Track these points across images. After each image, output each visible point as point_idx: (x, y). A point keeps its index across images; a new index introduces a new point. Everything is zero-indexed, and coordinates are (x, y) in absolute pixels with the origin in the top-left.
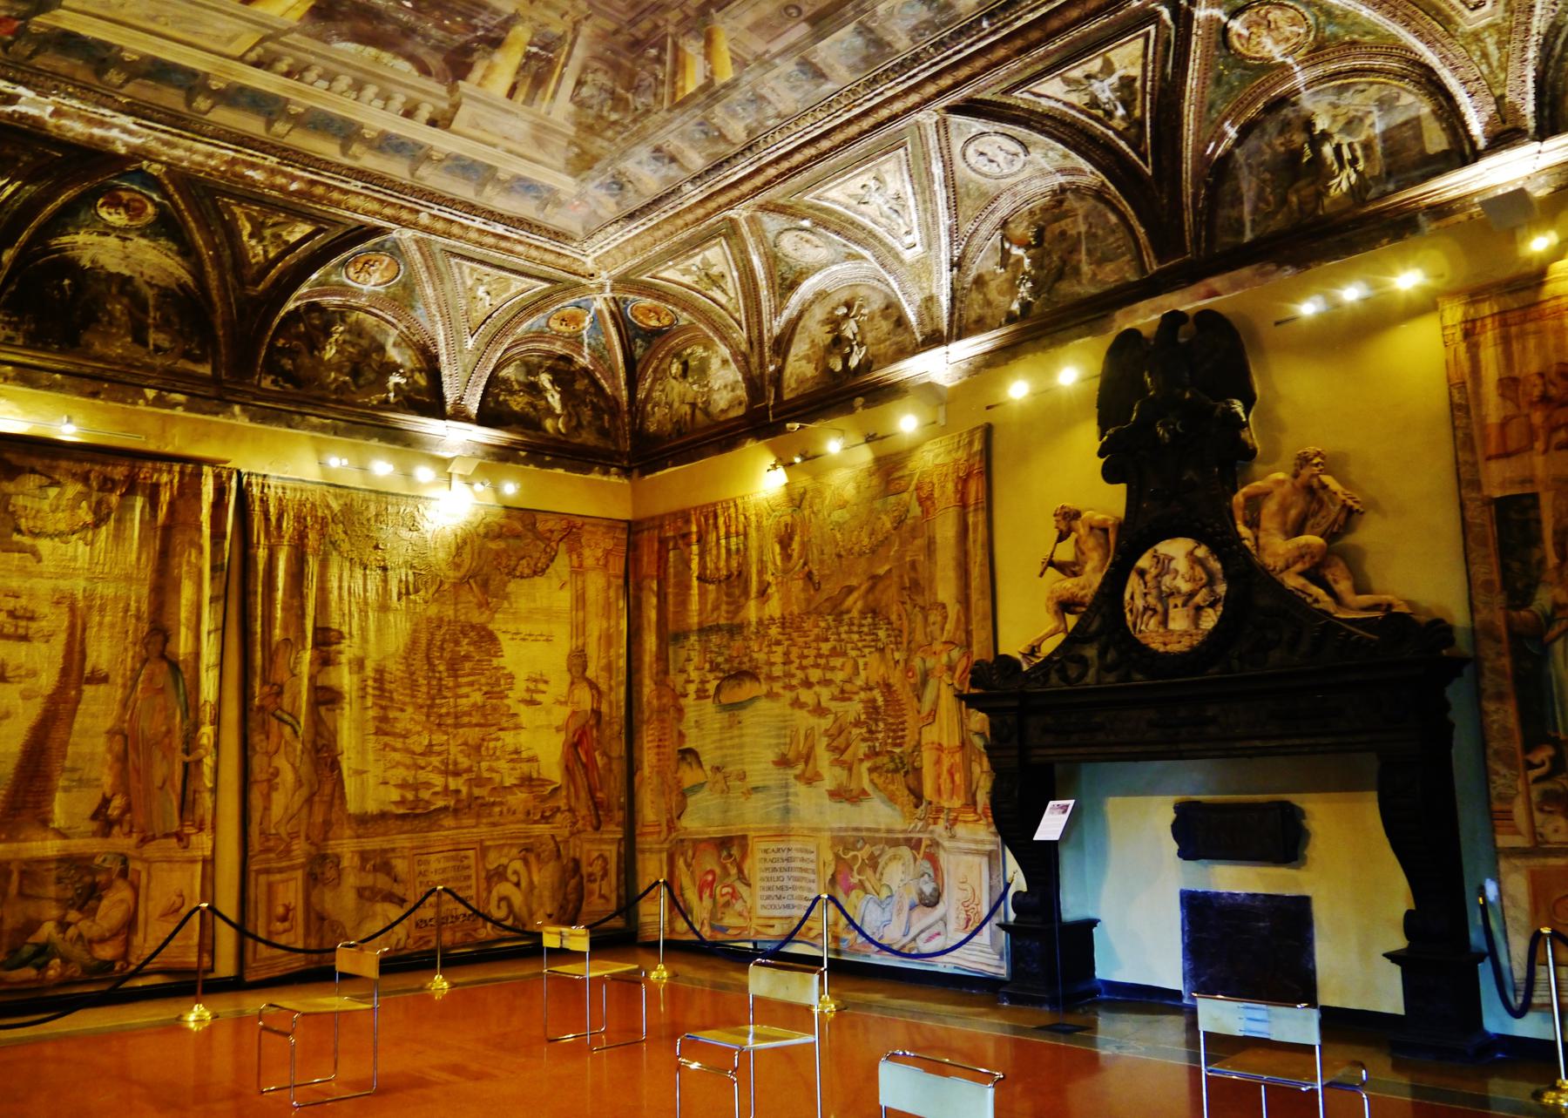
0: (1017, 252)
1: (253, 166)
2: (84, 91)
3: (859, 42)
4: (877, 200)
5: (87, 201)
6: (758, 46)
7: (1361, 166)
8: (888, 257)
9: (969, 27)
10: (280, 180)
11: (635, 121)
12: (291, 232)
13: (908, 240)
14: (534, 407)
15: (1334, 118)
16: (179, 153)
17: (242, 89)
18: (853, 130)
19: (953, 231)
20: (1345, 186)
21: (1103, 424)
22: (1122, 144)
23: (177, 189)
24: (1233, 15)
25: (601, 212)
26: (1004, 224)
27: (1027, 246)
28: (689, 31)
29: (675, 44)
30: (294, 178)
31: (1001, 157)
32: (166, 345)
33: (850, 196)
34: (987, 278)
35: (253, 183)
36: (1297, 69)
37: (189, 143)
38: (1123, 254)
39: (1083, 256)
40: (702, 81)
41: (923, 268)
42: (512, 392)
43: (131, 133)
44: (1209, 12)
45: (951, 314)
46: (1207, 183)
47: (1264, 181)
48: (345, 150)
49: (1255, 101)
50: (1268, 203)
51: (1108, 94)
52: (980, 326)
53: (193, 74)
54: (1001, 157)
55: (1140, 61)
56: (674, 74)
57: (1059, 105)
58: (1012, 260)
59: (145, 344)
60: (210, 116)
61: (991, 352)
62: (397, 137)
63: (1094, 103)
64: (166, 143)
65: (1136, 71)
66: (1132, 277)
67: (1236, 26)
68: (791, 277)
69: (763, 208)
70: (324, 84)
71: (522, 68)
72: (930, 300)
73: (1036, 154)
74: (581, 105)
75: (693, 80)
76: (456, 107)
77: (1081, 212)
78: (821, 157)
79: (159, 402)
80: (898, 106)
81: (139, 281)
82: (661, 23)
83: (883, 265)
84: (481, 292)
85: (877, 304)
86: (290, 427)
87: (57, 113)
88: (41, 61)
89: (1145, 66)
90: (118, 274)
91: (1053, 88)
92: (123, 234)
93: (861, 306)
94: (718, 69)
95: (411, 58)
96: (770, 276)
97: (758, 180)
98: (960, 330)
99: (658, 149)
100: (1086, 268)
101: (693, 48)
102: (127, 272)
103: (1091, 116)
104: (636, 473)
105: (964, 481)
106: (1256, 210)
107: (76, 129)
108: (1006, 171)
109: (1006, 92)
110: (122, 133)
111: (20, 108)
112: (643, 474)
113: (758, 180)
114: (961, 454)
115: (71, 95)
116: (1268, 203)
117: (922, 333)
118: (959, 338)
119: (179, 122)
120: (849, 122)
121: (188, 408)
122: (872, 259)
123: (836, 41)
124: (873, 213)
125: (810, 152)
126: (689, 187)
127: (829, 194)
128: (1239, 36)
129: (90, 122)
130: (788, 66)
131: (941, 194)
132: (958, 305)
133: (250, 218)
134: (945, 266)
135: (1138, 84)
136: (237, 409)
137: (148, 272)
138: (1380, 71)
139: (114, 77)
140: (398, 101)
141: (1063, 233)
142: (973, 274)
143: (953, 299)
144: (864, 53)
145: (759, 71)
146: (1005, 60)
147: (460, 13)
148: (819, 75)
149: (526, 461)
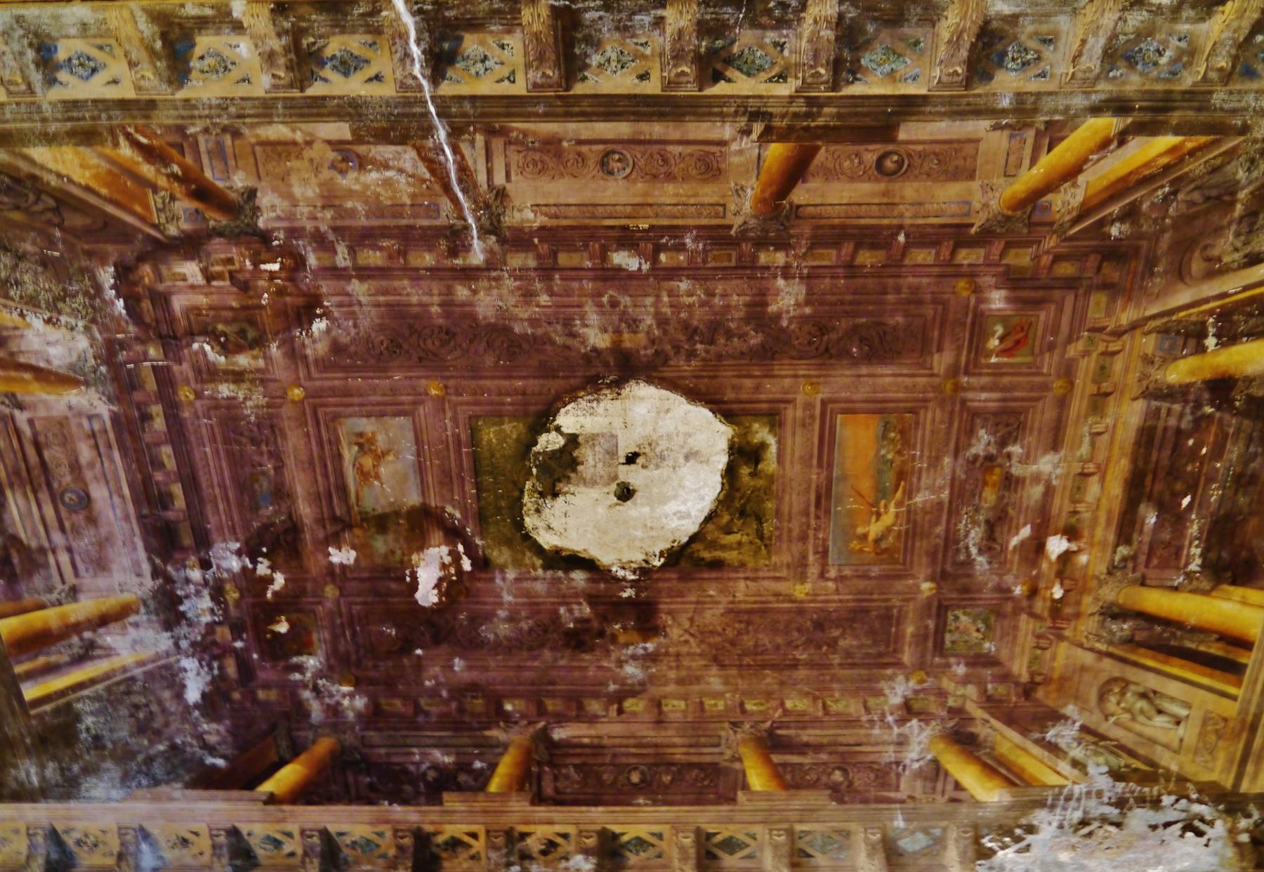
82: (1046, 260)
101: (1066, 201)
130: (1007, 84)
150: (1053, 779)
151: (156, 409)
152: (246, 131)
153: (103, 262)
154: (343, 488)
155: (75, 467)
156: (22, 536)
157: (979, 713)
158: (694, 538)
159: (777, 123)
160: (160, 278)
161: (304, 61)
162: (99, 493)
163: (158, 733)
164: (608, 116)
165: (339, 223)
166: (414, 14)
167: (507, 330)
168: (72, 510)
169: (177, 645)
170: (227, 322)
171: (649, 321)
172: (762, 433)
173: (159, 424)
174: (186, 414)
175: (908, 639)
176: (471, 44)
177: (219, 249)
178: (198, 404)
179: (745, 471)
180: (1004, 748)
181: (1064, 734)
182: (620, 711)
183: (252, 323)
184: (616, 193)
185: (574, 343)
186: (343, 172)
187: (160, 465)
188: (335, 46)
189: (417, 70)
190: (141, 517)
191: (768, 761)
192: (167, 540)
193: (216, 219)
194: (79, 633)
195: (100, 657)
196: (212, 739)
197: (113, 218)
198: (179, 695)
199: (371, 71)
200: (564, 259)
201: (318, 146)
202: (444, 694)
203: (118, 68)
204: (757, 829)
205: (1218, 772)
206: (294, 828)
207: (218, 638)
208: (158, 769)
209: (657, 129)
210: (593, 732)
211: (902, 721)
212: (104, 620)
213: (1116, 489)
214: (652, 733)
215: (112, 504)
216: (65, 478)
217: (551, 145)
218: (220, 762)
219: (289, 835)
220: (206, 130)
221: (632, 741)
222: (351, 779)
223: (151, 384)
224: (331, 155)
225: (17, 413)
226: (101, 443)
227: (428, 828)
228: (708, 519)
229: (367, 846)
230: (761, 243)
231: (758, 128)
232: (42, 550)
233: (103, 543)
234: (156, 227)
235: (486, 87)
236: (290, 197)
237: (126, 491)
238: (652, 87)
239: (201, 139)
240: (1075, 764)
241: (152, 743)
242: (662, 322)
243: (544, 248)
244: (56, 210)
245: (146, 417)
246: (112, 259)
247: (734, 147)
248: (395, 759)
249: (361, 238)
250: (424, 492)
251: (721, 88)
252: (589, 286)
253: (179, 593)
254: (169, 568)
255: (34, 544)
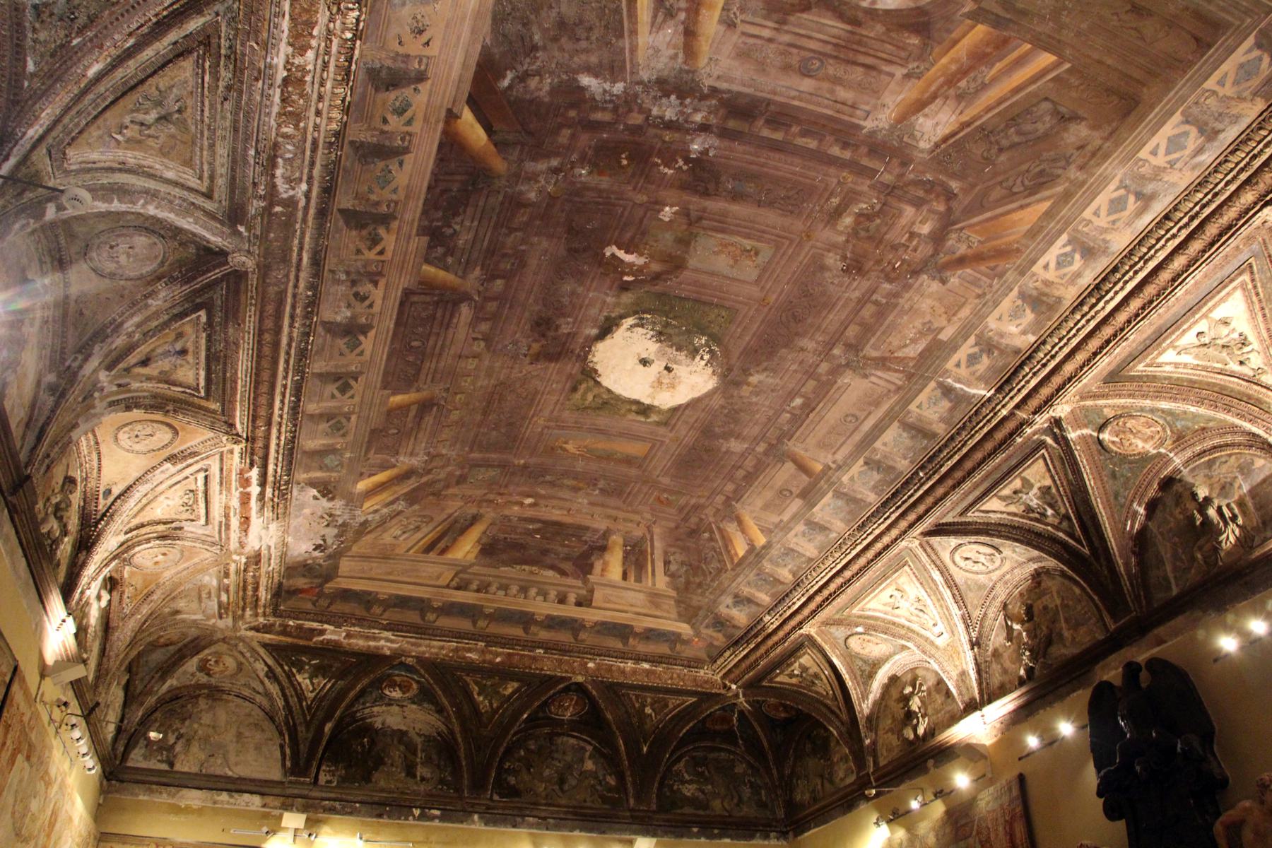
0: (1017, 627)
1: (469, 650)
2: (360, 621)
3: (840, 503)
4: (903, 604)
5: (377, 684)
6: (775, 519)
7: (1240, 521)
8: (926, 645)
9: (911, 478)
10: (489, 657)
11: (713, 580)
12: (506, 688)
13: (937, 630)
14: (703, 792)
15: (1211, 487)
16: (423, 649)
17: (453, 604)
18: (862, 561)
19: (967, 620)
20: (1232, 539)
21: (1099, 767)
22: (1061, 534)
23: (426, 671)
24: (1101, 428)
25: (716, 643)
26: (1005, 606)
27: (1022, 622)
28: (724, 518)
29: (719, 528)
30: (497, 655)
31: (982, 559)
32: (429, 775)
33: (885, 605)
34: (1001, 650)
35: (472, 662)
36: (1171, 455)
37: (427, 642)
38: (1090, 618)
39: (1063, 625)
40: (747, 547)
41: (952, 649)
42: (683, 782)
43: (392, 641)
44: (1079, 432)
45: (980, 684)
46: (1134, 553)
47: (1175, 544)
48: (526, 630)
49: (1150, 484)
50: (1182, 561)
51: (1035, 501)
52: (1002, 691)
53: (421, 600)
54: (982, 559)
55: (1047, 475)
56: (726, 546)
57: (1005, 516)
58: (1015, 634)
59: (414, 776)
60: (437, 624)
61: (1014, 711)
62: (558, 617)
63: (1029, 509)
64: (413, 644)
65: (1048, 482)
66: (1100, 637)
67: (1106, 436)
68: (868, 669)
69: (826, 623)
70: (501, 593)
71: (625, 558)
72: (963, 674)
73: (1007, 552)
74: (673, 576)
75: (741, 549)
76: (592, 591)
77: (1054, 589)
78: (848, 582)
79: (423, 817)
80: (886, 540)
81: (412, 734)
83: (924, 652)
84: (648, 710)
85: (931, 681)
86: (514, 826)
87: (349, 636)
88: (333, 608)
89: (1052, 477)
90: (400, 731)
91: (993, 504)
92: (399, 703)
93: (921, 685)
94: (753, 537)
95: (552, 567)
96: (851, 672)
97: (812, 606)
98: (989, 695)
99: (736, 596)
100: (1066, 634)
101: (731, 528)
102: (404, 728)
103: (1031, 519)
104: (791, 834)
105: (1010, 823)
106: (1175, 569)
107: (360, 643)
108: (991, 568)
109: (961, 515)
110: (386, 642)
111: (327, 636)
112: (796, 836)
113: (812, 606)
114: (1005, 799)
115: (354, 625)
116: (1182, 561)
117: (963, 702)
118: (990, 702)
119: (422, 631)
120: (858, 556)
121: (442, 819)
122: (915, 649)
123: (824, 506)
124: (904, 613)
125: (839, 581)
126: (767, 618)
127: (868, 606)
128: (1113, 442)
129: (368, 638)
130: (801, 527)
131: (947, 594)
132: (984, 675)
133: (476, 683)
134: (967, 647)
135: (1054, 490)
136: (476, 817)
137: (418, 726)
138: (1233, 445)
139: (377, 610)
140: (553, 594)
141: (1045, 608)
142: (991, 649)
143: (979, 672)
144: (847, 509)
145: (781, 534)
146: (946, 495)
147: (573, 535)
148: (823, 529)
149: (698, 836)
150: (366, 505)
151: (847, 155)
152: (977, 301)
153: (961, 189)
154: (723, 231)
155: (837, 81)
156: (805, 16)
157: (424, 479)
158: (598, 384)
159: (830, 473)
160: (931, 211)
161: (988, 346)
162: (807, 85)
163: (555, 39)
164: (875, 426)
165: (899, 308)
166: (974, 396)
167: (786, 346)
168: (804, 61)
169: (640, 83)
170: (878, 226)
171: (754, 399)
172: (654, 418)
173: (836, 151)
174: (832, 170)
175: (487, 455)
176: (946, 404)
177: (925, 250)
178: (835, 181)
179: (634, 408)
180: (396, 488)
181: (401, 506)
182: (474, 339)
183: (869, 238)
184: (832, 415)
185: (760, 368)
186: (924, 324)
187: (805, 133)
188: (985, 361)
189: (949, 380)
190: (769, 102)
191: (414, 403)
192: (740, 112)
193: (943, 258)
194: (687, 10)
195: (655, 16)
196: (533, 83)
197: (981, 214)
198: (589, 70)
199: (963, 365)
200: (812, 384)
201: (944, 323)
202: (523, 248)
203: (1051, 275)
204: (357, 399)
205: (355, 549)
206: (416, 127)
207: (635, 115)
208: (512, 28)
209: (857, 437)
210: (462, 323)
211: (428, 454)
212: (690, 34)
213: (555, 518)
214: (452, 352)
215: (793, 89)
216: (832, 69)
217: (877, 404)
218: (506, 83)
219: (409, 123)
220: (991, 286)
221: (448, 343)
222: (458, 178)
223: (865, 162)
224: (936, 325)
225: (905, 71)
226: (846, 108)
227: (395, 225)
228: (609, 391)
229: (385, 180)
230: (771, 446)
231: (833, 466)
232: (783, 22)
233: (762, 67)
234: (962, 229)
235: (922, 397)
236: (929, 296)
237: (796, 103)
238: (878, 444)
239: (989, 281)
240: (376, 511)
241: (545, 31)
242: (750, 404)
243: (824, 378)
244: (1010, 189)
245: (845, 145)
246: (961, 196)
247: (830, 456)
248: (470, 210)
249: (881, 313)
250: (696, 270)
251: (861, 461)
252: (791, 386)
253: (688, 101)
254: (714, 102)
255: (792, 19)
